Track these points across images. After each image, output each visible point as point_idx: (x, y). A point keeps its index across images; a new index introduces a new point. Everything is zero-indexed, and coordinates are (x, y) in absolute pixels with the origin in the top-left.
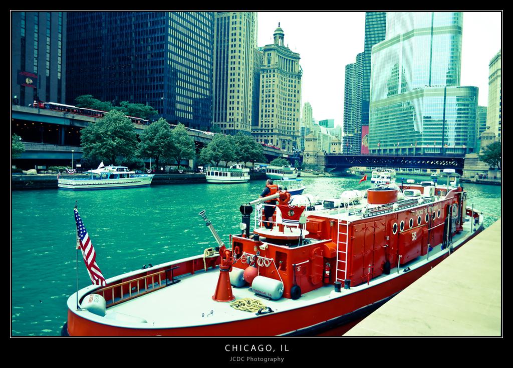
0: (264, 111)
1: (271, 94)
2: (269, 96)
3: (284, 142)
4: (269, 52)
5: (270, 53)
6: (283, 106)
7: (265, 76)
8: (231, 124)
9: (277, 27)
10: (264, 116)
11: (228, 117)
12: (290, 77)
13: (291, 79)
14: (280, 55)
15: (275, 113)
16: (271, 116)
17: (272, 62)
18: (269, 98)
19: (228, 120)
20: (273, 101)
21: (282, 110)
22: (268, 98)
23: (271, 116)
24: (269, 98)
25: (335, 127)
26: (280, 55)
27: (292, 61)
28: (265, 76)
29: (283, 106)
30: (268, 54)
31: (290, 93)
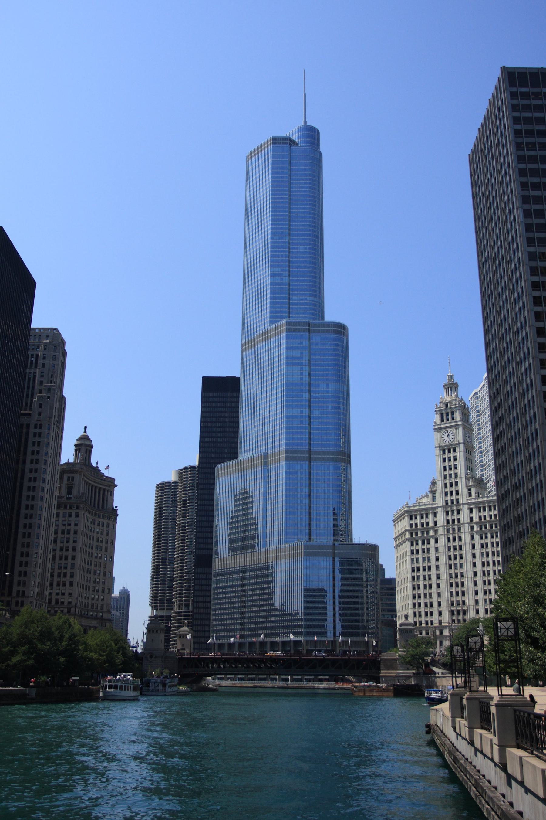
0: (56, 574)
4: (71, 475)
5: (73, 478)
6: (87, 566)
8: (20, 600)
11: (15, 588)
12: (99, 517)
13: (101, 520)
14: (88, 481)
15: (77, 579)
16: (68, 584)
17: (75, 492)
18: (67, 553)
19: (14, 594)
20: (73, 558)
22: (64, 553)
23: (68, 584)
24: (67, 553)
26: (88, 481)
27: (104, 490)
29: (87, 566)
30: (69, 478)
31: (99, 544)
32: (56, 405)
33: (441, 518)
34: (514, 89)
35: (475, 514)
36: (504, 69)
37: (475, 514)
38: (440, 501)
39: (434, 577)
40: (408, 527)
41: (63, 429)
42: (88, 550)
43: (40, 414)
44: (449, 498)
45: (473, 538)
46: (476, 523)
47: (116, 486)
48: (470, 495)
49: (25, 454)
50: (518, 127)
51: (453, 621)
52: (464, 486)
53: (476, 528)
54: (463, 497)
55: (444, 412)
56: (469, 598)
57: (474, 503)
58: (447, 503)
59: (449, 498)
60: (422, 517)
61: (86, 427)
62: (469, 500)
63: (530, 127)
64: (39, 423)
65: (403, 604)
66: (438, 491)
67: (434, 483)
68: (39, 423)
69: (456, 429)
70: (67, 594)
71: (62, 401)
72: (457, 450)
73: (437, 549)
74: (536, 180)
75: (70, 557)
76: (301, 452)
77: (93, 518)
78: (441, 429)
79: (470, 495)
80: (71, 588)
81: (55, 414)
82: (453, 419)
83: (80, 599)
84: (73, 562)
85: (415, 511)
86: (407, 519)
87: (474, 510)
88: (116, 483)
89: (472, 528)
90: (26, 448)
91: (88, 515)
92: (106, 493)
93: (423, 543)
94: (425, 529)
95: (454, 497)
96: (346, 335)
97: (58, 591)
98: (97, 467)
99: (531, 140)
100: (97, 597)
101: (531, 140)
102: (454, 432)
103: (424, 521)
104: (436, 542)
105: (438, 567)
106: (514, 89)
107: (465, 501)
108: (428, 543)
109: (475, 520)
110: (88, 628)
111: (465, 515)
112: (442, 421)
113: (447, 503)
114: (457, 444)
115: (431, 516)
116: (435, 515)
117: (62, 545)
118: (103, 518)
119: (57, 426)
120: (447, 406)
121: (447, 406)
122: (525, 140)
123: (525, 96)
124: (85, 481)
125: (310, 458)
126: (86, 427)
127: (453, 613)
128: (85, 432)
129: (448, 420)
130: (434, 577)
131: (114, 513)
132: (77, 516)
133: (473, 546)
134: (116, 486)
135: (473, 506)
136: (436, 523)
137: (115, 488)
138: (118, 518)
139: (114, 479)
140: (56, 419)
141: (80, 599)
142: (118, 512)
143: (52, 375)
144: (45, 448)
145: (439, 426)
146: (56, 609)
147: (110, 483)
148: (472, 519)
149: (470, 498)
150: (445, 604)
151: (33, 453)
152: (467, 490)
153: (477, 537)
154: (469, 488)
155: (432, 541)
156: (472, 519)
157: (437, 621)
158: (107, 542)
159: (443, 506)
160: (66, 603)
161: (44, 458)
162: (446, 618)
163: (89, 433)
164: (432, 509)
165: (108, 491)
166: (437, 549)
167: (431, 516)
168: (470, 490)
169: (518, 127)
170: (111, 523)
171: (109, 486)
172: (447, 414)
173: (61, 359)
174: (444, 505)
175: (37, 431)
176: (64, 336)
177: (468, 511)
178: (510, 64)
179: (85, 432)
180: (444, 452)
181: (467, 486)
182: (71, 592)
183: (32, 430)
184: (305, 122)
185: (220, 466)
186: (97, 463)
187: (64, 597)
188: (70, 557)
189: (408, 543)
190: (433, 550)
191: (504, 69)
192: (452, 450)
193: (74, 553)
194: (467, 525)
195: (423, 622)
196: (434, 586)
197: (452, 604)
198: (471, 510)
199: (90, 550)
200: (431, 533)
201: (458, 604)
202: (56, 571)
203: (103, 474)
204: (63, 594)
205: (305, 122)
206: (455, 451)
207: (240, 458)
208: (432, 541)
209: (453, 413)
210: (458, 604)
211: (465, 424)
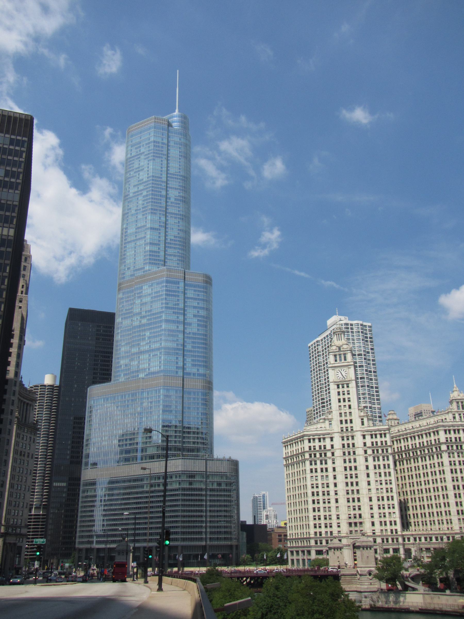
13: (25, 434)
27: (28, 404)
33: (338, 442)
35: (368, 440)
37: (368, 440)
39: (332, 493)
40: (307, 449)
44: (344, 425)
45: (366, 461)
46: (369, 447)
48: (363, 423)
52: (357, 416)
53: (369, 452)
54: (357, 425)
56: (366, 512)
57: (367, 431)
58: (342, 431)
59: (344, 425)
62: (363, 428)
66: (334, 419)
69: (349, 368)
72: (350, 385)
78: (335, 367)
79: (363, 423)
82: (345, 359)
86: (306, 442)
87: (366, 437)
89: (366, 452)
93: (321, 463)
94: (323, 451)
95: (349, 425)
102: (347, 370)
103: (322, 444)
105: (335, 485)
107: (358, 429)
108: (326, 463)
111: (359, 441)
112: (336, 361)
113: (342, 431)
114: (350, 381)
115: (328, 441)
116: (332, 439)
120: (339, 348)
121: (339, 348)
127: (350, 524)
129: (341, 360)
130: (332, 493)
133: (367, 467)
135: (365, 433)
136: (332, 446)
148: (365, 444)
149: (363, 426)
150: (344, 517)
152: (360, 420)
154: (362, 418)
156: (365, 444)
159: (339, 432)
162: (345, 528)
164: (329, 434)
165: (30, 405)
167: (328, 441)
168: (362, 419)
172: (340, 355)
174: (340, 431)
177: (362, 437)
180: (338, 387)
181: (360, 416)
186: (22, 378)
189: (308, 463)
190: (330, 470)
192: (345, 386)
194: (361, 449)
196: (333, 501)
197: (350, 518)
198: (364, 437)
200: (329, 454)
201: (355, 517)
206: (348, 387)
208: (330, 462)
209: (345, 354)
210: (355, 517)
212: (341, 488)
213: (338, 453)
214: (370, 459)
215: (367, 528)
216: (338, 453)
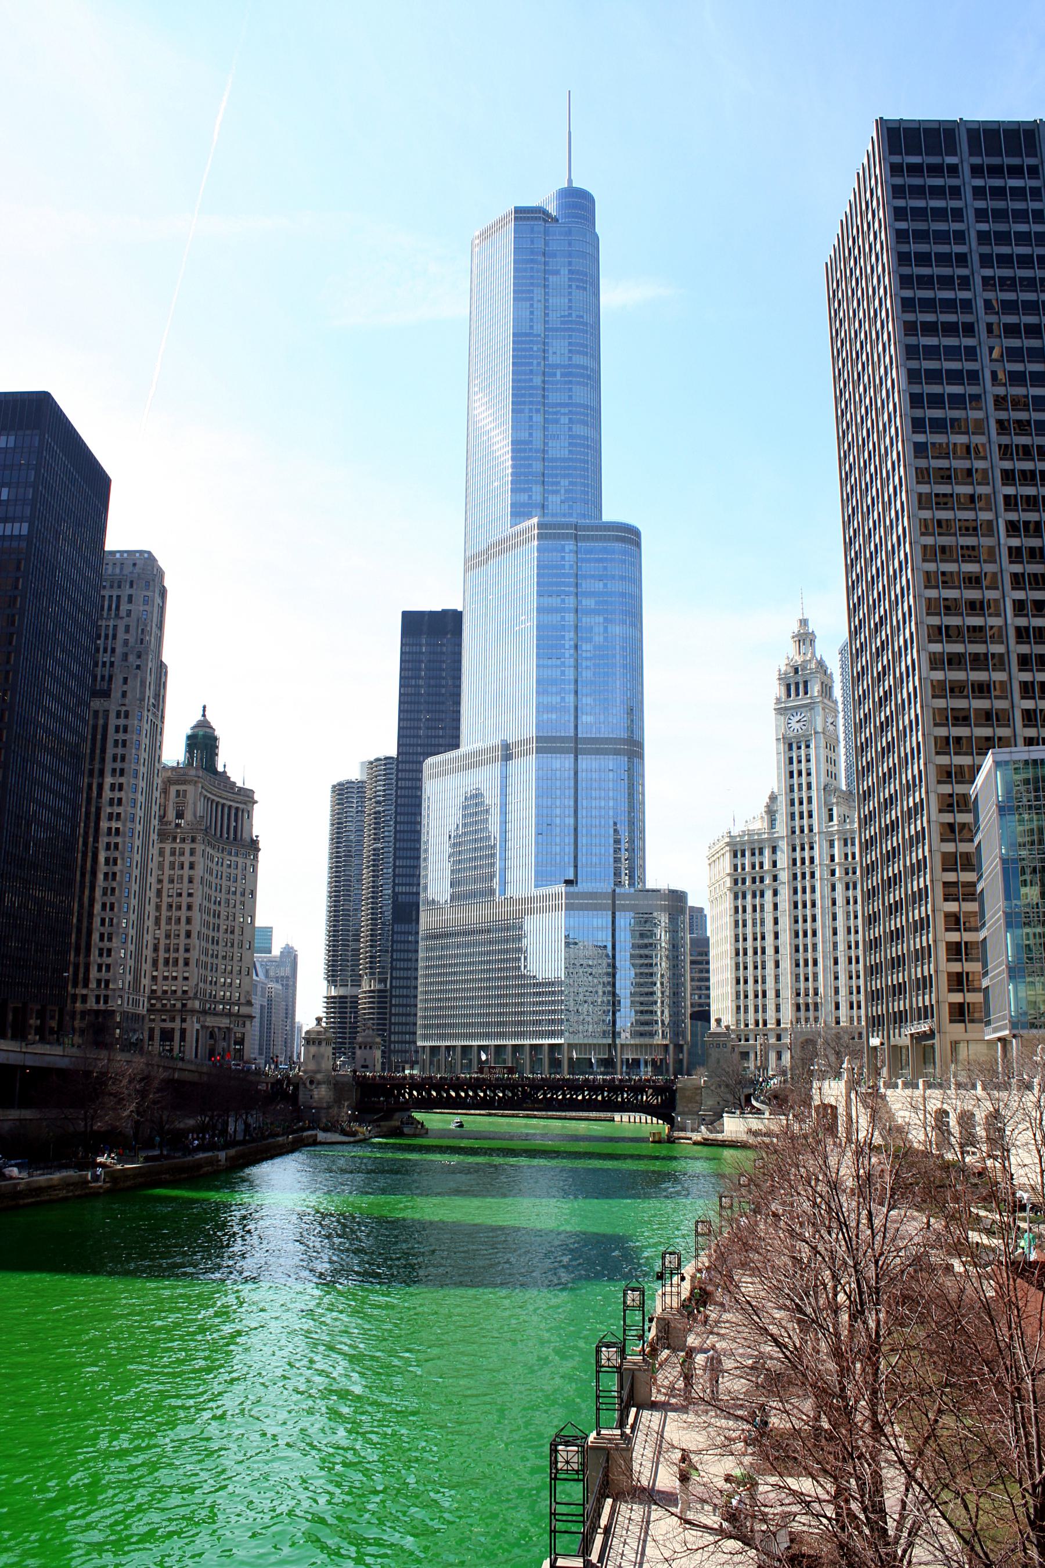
0: (162, 947)
1: (184, 900)
2: (179, 908)
3: (212, 1035)
4: (181, 788)
5: (185, 791)
6: (211, 934)
7: (168, 852)
9: (199, 717)
10: (161, 961)
11: (94, 973)
12: (230, 854)
13: (233, 859)
14: (209, 795)
15: (194, 955)
16: (181, 962)
19: (93, 985)
21: (210, 946)
22: (175, 913)
23: (181, 962)
24: (179, 913)
25: (276, 951)
26: (209, 795)
27: (237, 809)
28: (168, 852)
29: (211, 934)
30: (178, 791)
32: (151, 679)
34: (897, 159)
36: (881, 123)
38: (782, 828)
41: (163, 717)
42: (213, 907)
43: (124, 694)
45: (833, 888)
47: (256, 802)
49: (103, 760)
50: (903, 225)
51: (798, 1020)
55: (792, 681)
60: (753, 854)
61: (204, 707)
63: (921, 226)
64: (124, 708)
65: (720, 991)
67: (773, 798)
68: (124, 708)
70: (180, 979)
71: (161, 669)
73: (775, 906)
74: (930, 318)
75: (183, 920)
76: (563, 739)
77: (220, 855)
78: (786, 709)
80: (187, 969)
81: (149, 693)
82: (806, 693)
83: (201, 985)
84: (188, 927)
85: (743, 843)
88: (256, 797)
90: (103, 751)
91: (211, 851)
92: (240, 813)
96: (638, 545)
97: (166, 974)
98: (225, 772)
99: (923, 248)
100: (229, 981)
101: (923, 248)
104: (775, 893)
106: (897, 159)
109: (837, 860)
110: (216, 1030)
112: (789, 695)
115: (767, 852)
116: (774, 850)
117: (170, 900)
118: (237, 855)
119: (154, 714)
121: (796, 671)
122: (914, 248)
123: (915, 170)
124: (205, 796)
125: (576, 749)
126: (204, 707)
127: (798, 1008)
128: (204, 715)
131: (253, 846)
132: (192, 852)
134: (256, 802)
137: (255, 806)
138: (260, 854)
139: (252, 792)
140: (152, 700)
141: (201, 985)
142: (261, 845)
143: (143, 630)
144: (134, 751)
145: (783, 705)
146: (165, 1002)
147: (247, 798)
151: (115, 759)
153: (840, 887)
155: (768, 894)
157: (774, 1021)
158: (243, 894)
160: (179, 993)
161: (133, 766)
162: (787, 1014)
163: (209, 717)
166: (775, 906)
167: (767, 852)
168: (831, 810)
169: (903, 225)
170: (249, 863)
171: (245, 804)
173: (158, 600)
175: (122, 722)
176: (162, 563)
178: (893, 114)
179: (204, 715)
182: (186, 975)
183: (113, 722)
184: (570, 181)
185: (430, 760)
187: (175, 983)
188: (183, 920)
191: (881, 123)
193: (189, 914)
195: (751, 1022)
196: (770, 965)
199: (217, 908)
202: (163, 942)
203: (234, 783)
204: (175, 978)
205: (570, 181)
207: (465, 748)
208: (768, 894)
211: (826, 701)
212: (785, 938)
213: (784, 876)
214: (840, 887)
215: (826, 1012)
216: (784, 876)
